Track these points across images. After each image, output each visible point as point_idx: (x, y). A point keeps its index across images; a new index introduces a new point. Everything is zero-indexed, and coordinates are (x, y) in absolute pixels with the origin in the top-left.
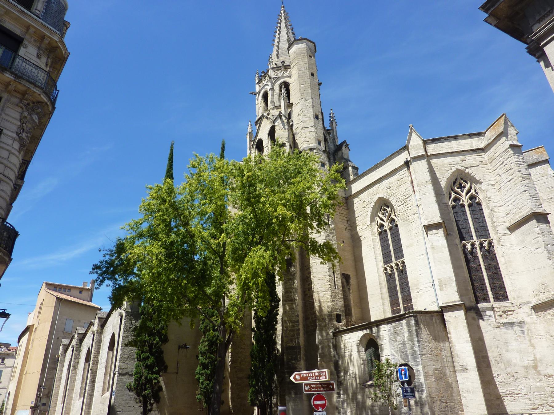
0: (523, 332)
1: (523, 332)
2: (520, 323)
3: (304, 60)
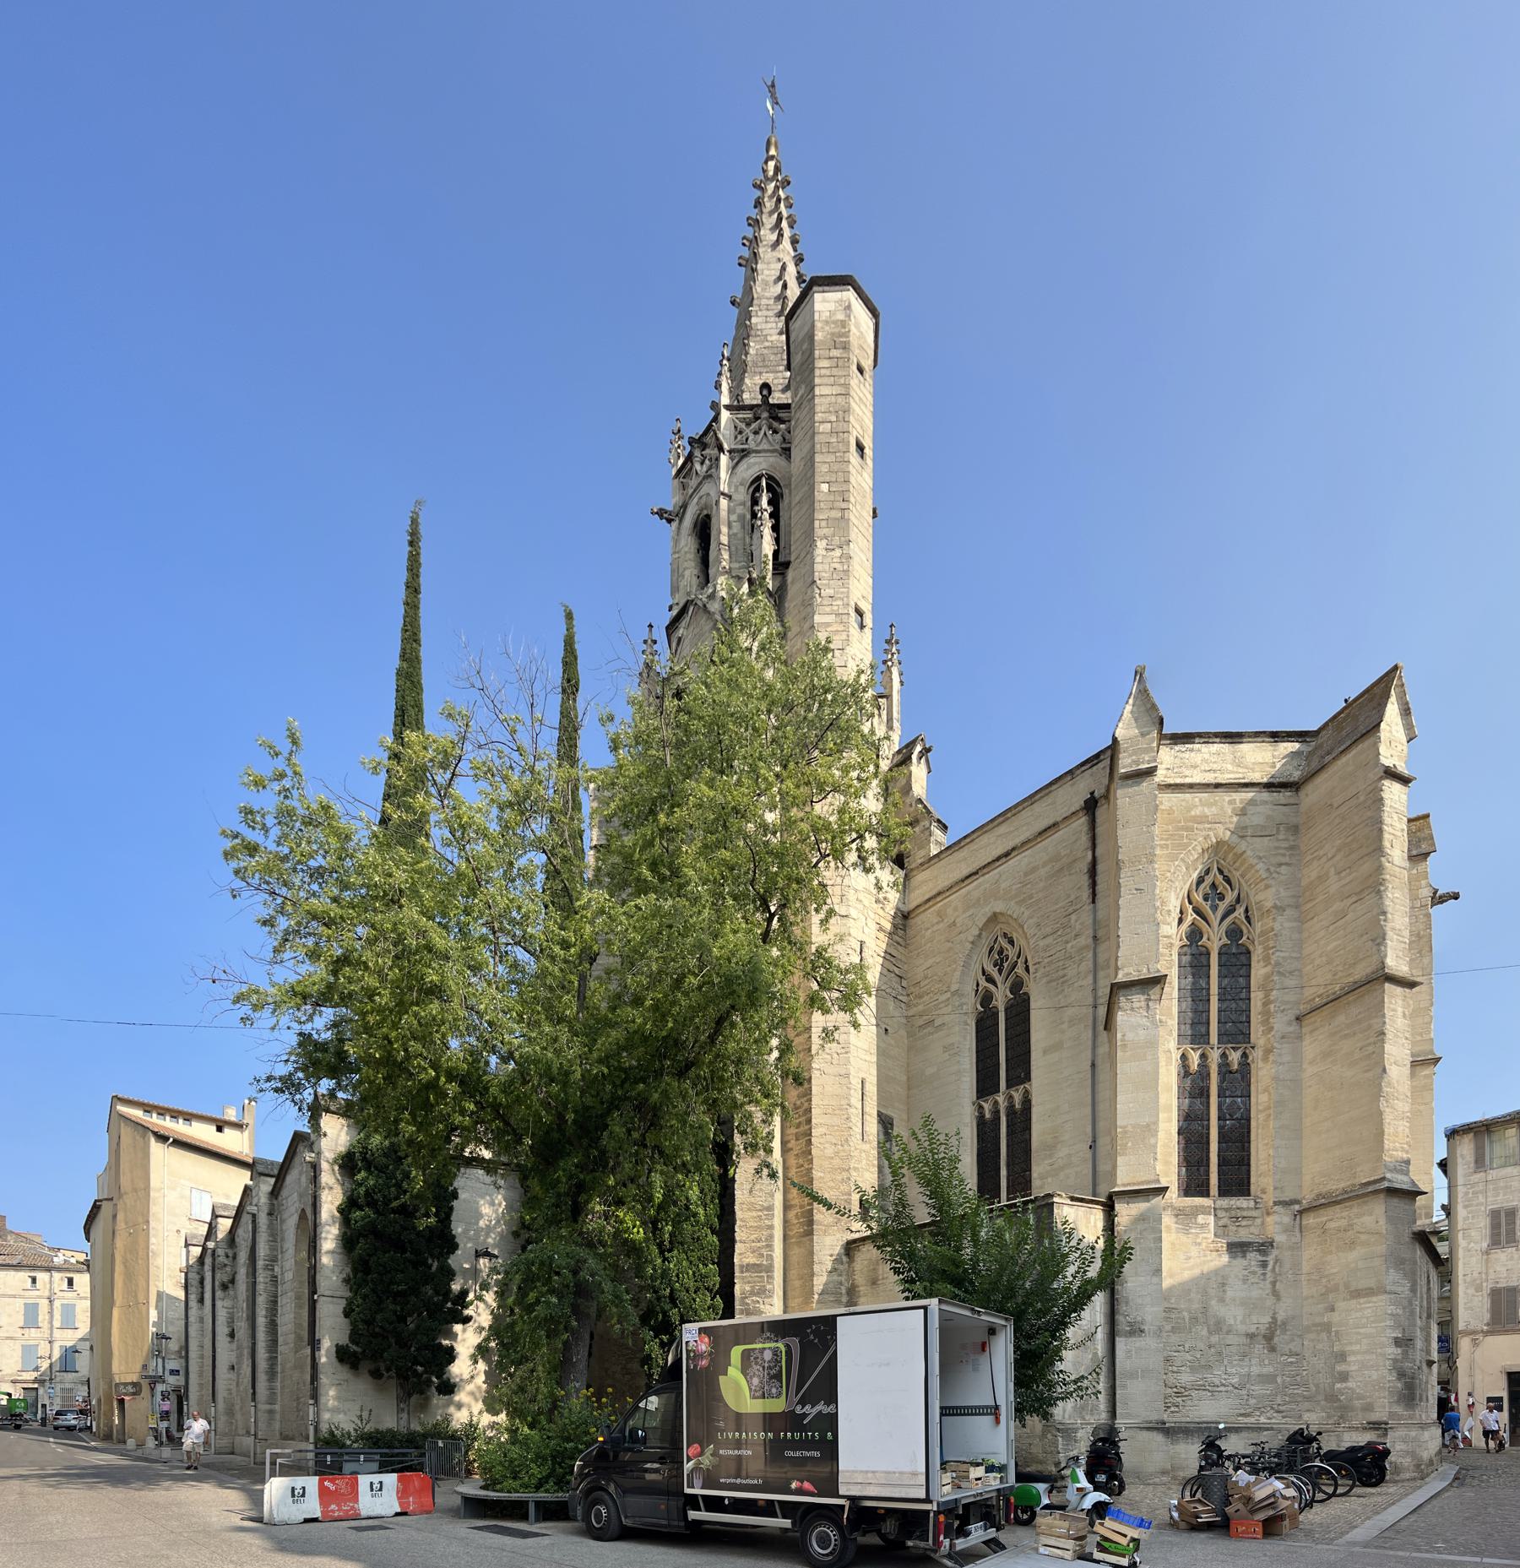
0: (1264, 1265)
1: (1264, 1265)
2: (1262, 1245)
3: (840, 377)
